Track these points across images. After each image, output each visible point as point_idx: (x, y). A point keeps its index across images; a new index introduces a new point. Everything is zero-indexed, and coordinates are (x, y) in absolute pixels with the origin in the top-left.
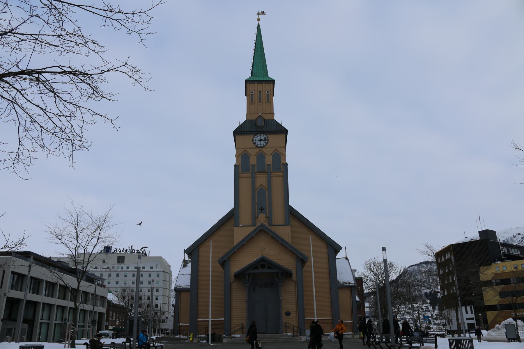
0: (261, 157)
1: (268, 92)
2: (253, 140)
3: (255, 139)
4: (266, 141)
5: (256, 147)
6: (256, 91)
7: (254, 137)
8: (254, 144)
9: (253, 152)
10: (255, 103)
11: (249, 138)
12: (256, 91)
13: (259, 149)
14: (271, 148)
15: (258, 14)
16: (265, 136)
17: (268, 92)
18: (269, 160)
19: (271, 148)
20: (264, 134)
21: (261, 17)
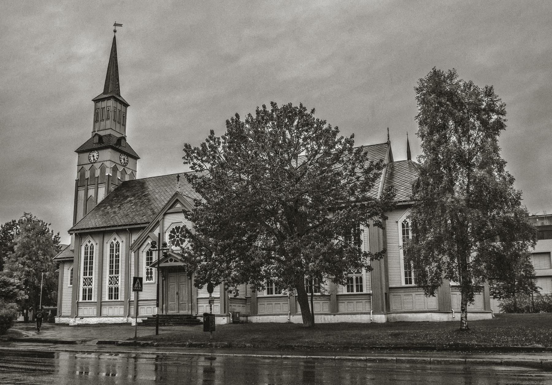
0: (92, 170)
1: (109, 108)
2: (89, 157)
3: (90, 156)
4: (98, 157)
5: (90, 163)
6: (100, 109)
7: (90, 154)
8: (89, 160)
9: (87, 167)
10: (104, 120)
11: (86, 155)
12: (100, 109)
13: (91, 165)
14: (100, 162)
15: (115, 25)
16: (97, 152)
17: (109, 108)
18: (98, 173)
19: (100, 162)
20: (97, 151)
21: (117, 28)
